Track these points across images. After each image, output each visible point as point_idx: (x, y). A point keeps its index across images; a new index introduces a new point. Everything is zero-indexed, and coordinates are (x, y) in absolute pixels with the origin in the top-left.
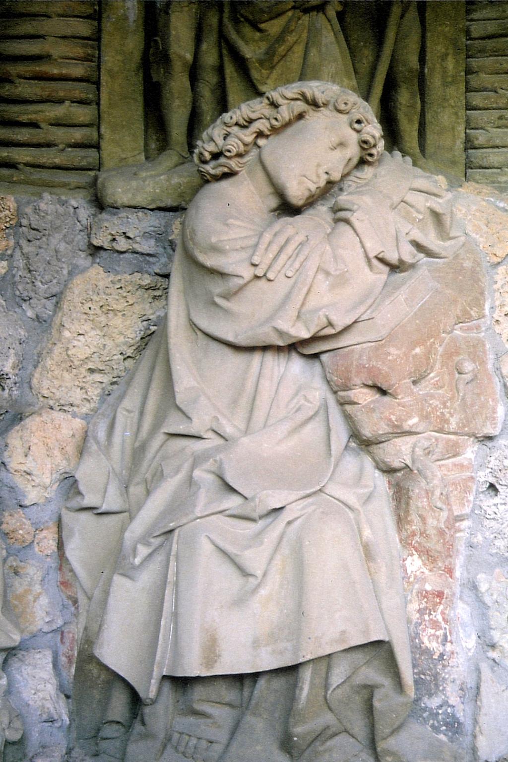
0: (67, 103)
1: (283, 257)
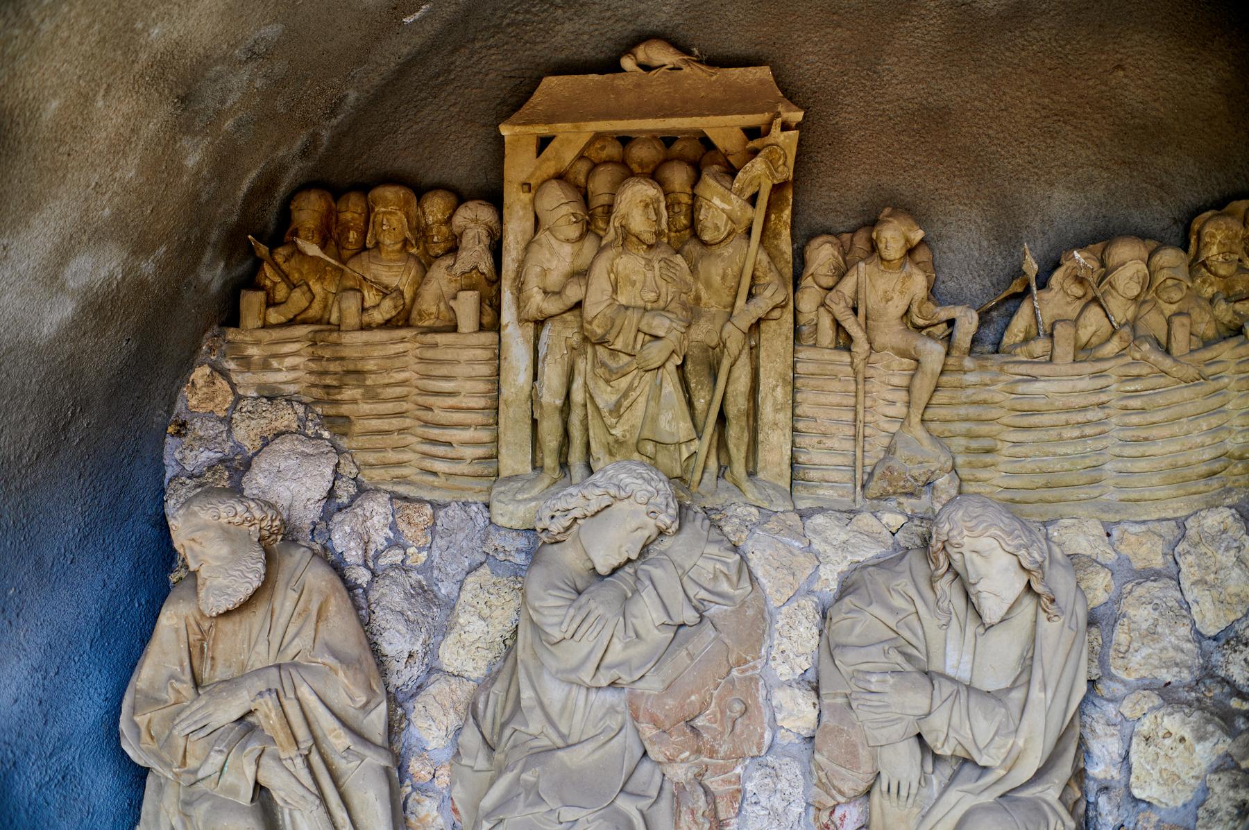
0: (472, 429)
1: (585, 626)
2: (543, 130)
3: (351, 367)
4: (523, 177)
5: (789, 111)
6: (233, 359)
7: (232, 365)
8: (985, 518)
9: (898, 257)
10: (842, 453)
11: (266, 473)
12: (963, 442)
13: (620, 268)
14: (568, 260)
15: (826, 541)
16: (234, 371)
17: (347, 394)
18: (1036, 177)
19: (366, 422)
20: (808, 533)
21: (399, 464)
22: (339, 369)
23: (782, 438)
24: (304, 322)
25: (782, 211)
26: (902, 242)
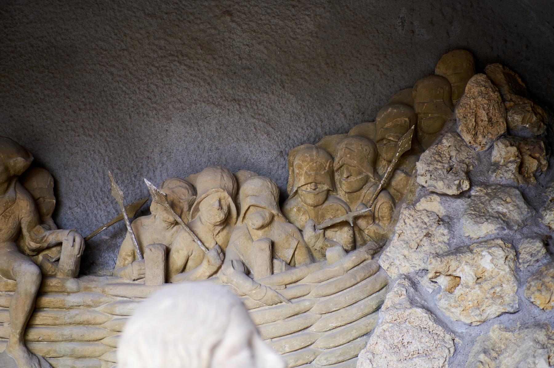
18: (155, 112)
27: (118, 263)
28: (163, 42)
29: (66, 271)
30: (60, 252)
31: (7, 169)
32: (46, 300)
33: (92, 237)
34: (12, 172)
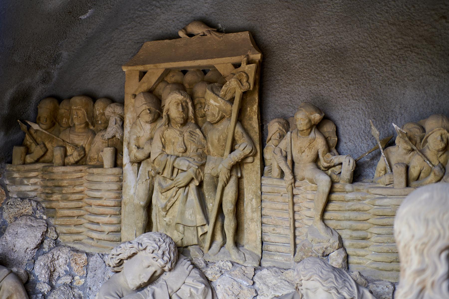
0: (108, 216)
2: (141, 68)
3: (57, 184)
4: (133, 92)
5: (253, 54)
6: (8, 179)
7: (7, 182)
8: (312, 270)
9: (305, 128)
10: (286, 236)
11: (11, 234)
12: (349, 232)
13: (167, 136)
14: (149, 132)
15: (265, 284)
16: (9, 185)
17: (55, 197)
18: (396, 83)
19: (62, 211)
20: (256, 279)
21: (78, 233)
22: (51, 185)
23: (256, 227)
24: (44, 162)
25: (253, 106)
26: (307, 121)
27: (375, 175)
28: (400, 40)
29: (345, 179)
30: (341, 168)
31: (310, 121)
32: (334, 196)
33: (359, 160)
34: (313, 123)
